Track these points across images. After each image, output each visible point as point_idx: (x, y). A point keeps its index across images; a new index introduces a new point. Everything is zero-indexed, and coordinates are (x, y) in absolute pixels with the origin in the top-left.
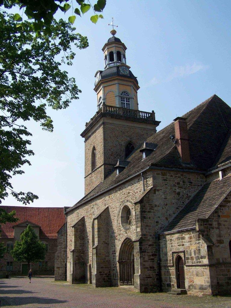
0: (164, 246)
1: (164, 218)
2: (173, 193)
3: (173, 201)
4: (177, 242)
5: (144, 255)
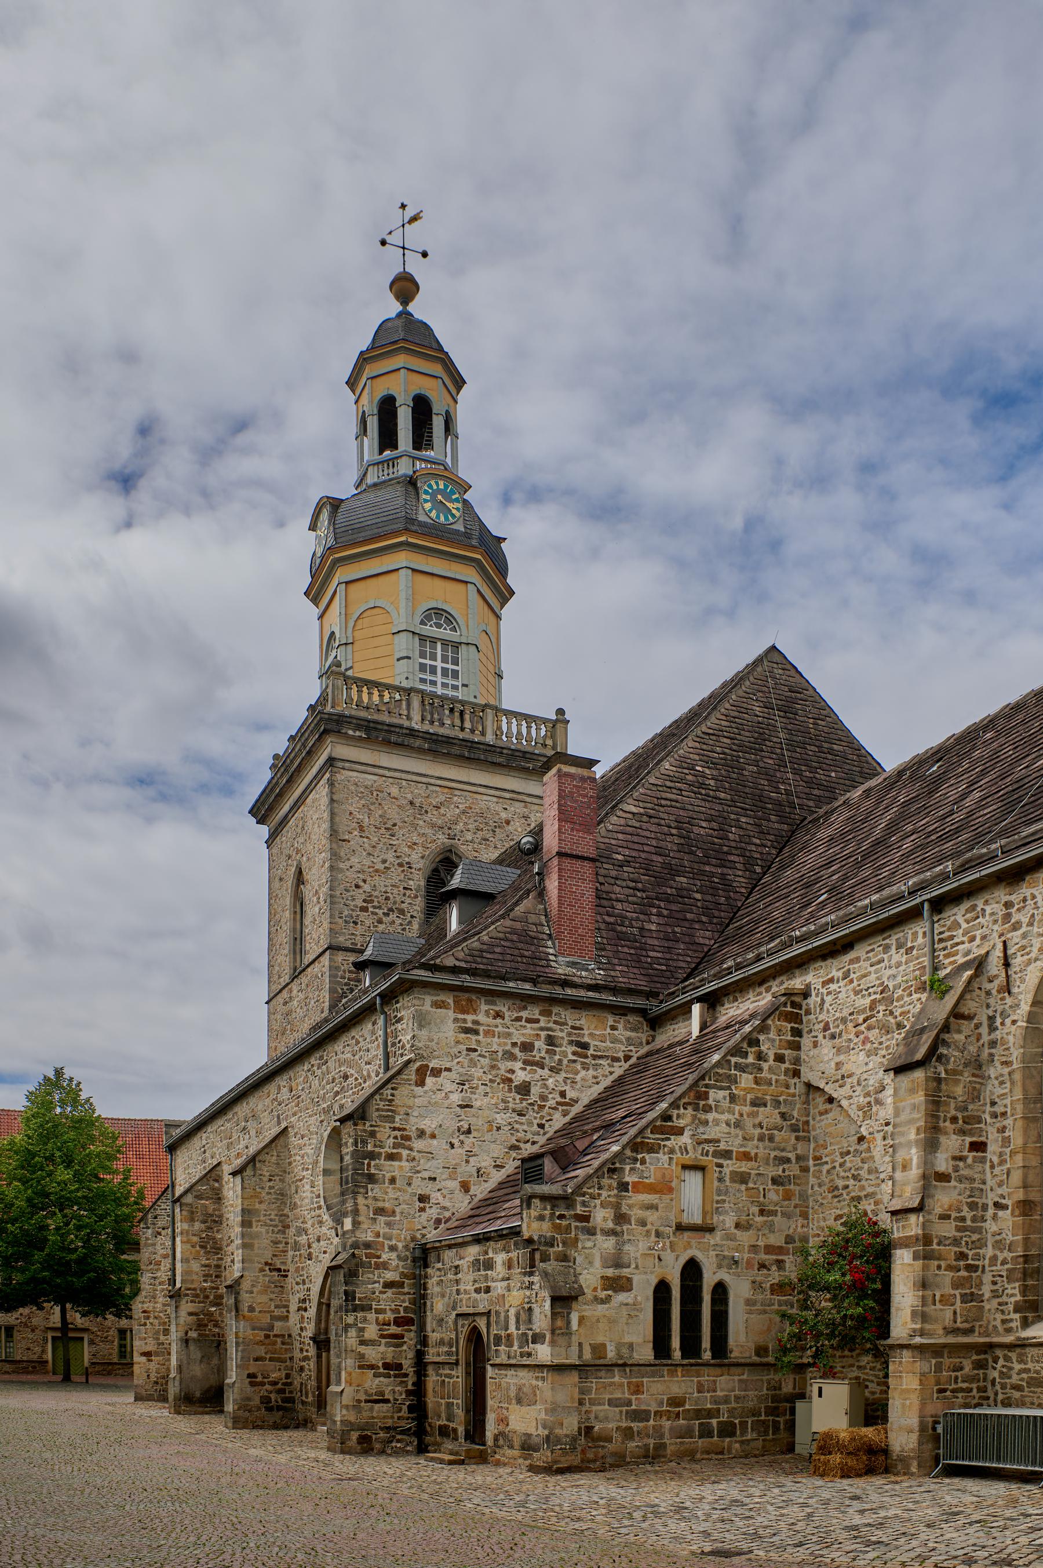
0: (437, 1289)
1: (454, 1185)
2: (502, 1085)
3: (501, 1118)
4: (471, 1277)
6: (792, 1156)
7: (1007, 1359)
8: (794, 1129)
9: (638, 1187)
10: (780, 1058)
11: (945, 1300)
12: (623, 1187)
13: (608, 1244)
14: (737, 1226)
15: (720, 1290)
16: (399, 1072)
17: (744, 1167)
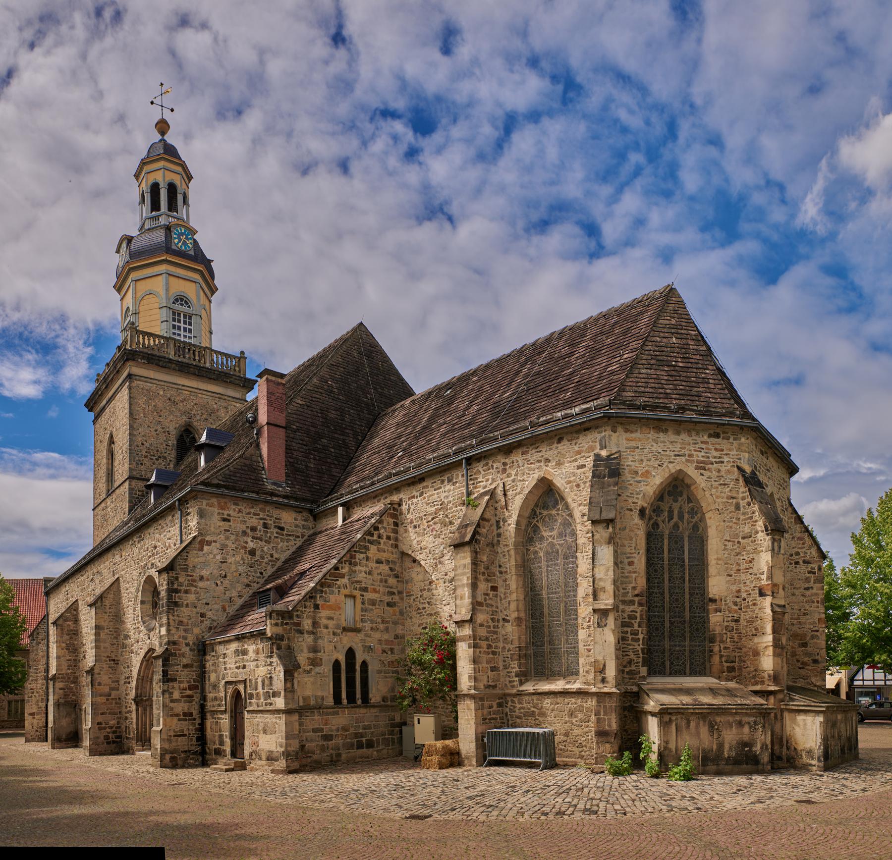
0: (212, 668)
10: (388, 538)
15: (364, 664)
16: (190, 543)
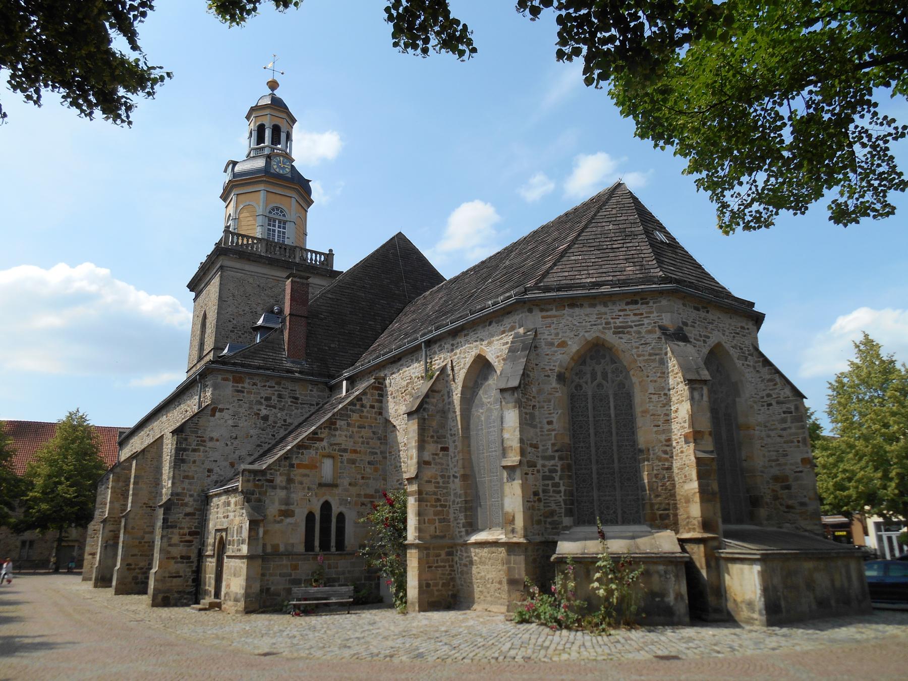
5: (172, 533)
6: (378, 451)
7: (461, 551)
8: (379, 439)
9: (300, 466)
11: (431, 522)
12: (292, 466)
13: (282, 494)
14: (350, 484)
17: (354, 456)
